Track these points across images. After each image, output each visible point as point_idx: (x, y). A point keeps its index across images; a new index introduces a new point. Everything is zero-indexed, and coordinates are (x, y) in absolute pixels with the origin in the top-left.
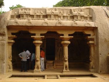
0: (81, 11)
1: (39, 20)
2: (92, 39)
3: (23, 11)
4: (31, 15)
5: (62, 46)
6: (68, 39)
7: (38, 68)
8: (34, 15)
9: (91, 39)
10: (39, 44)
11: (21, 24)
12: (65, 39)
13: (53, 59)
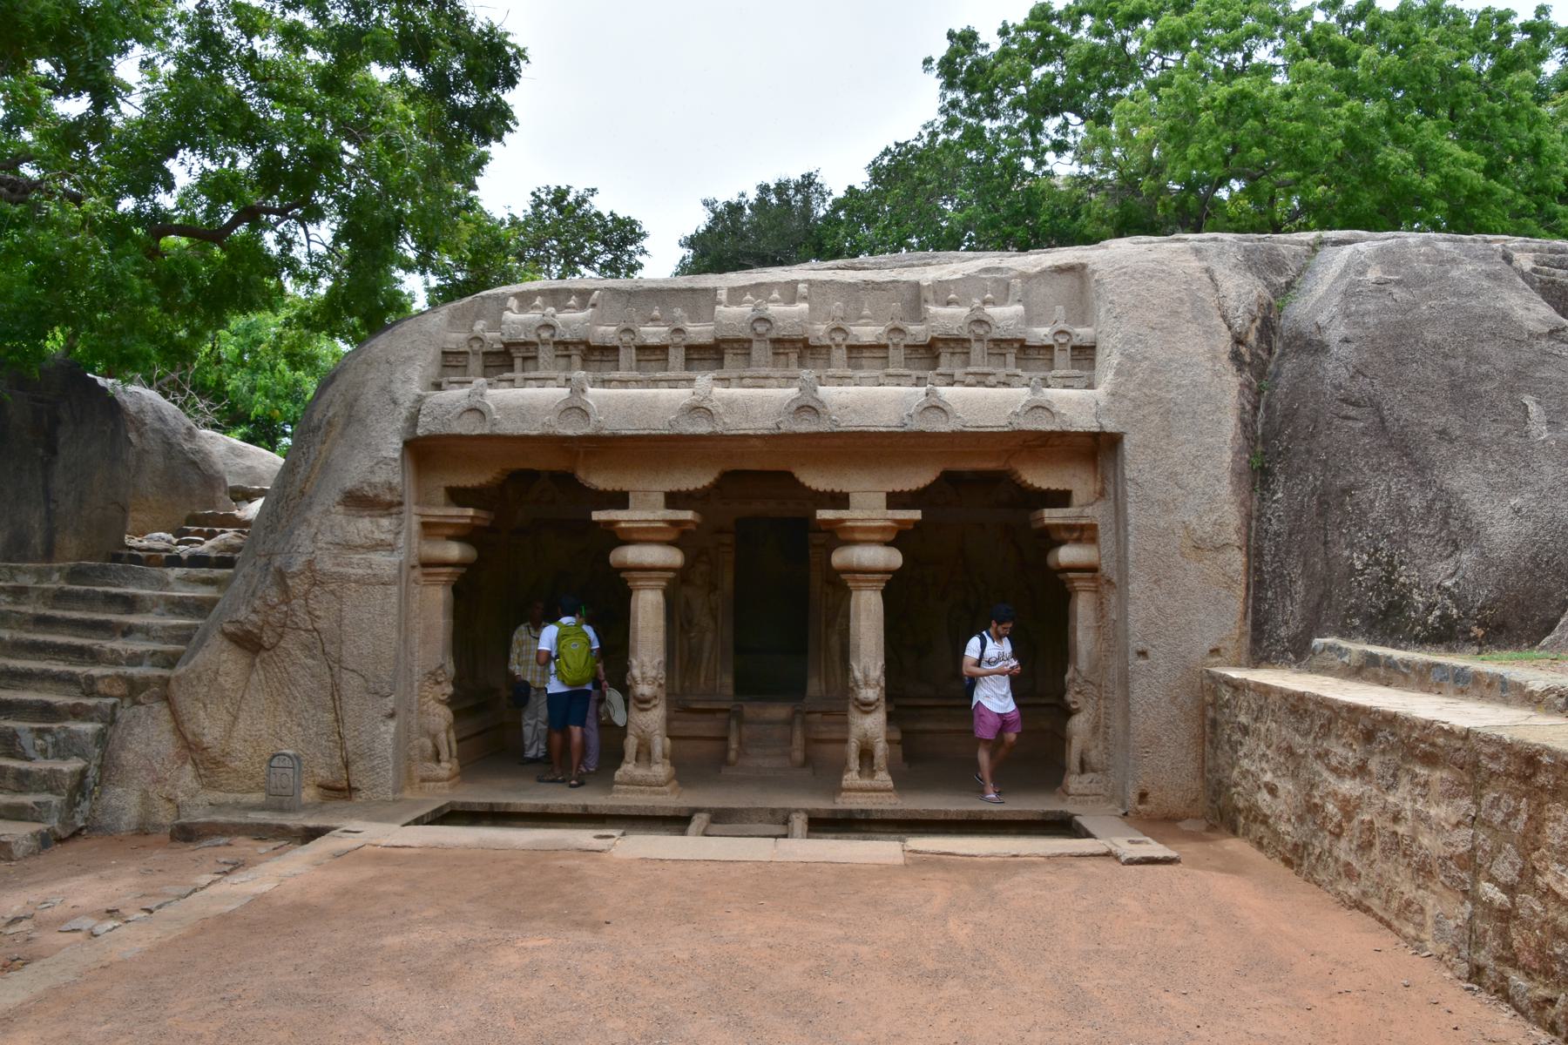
0: (1003, 292)
1: (650, 392)
2: (1084, 533)
3: (533, 316)
5: (840, 585)
6: (883, 529)
7: (645, 754)
8: (616, 343)
9: (1070, 528)
10: (654, 574)
11: (509, 428)
12: (853, 529)
13: (793, 689)
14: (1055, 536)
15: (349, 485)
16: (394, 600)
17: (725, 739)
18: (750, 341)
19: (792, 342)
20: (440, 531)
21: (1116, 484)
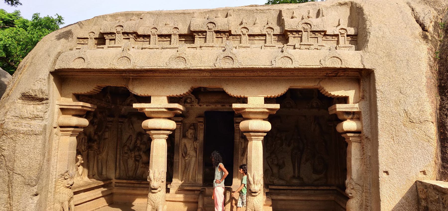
4: (140, 33)
6: (263, 113)
9: (348, 113)
10: (162, 132)
14: (340, 117)
15: (24, 91)
16: (40, 142)
17: (197, 203)
18: (206, 32)
19: (224, 32)
20: (69, 112)
21: (370, 93)
